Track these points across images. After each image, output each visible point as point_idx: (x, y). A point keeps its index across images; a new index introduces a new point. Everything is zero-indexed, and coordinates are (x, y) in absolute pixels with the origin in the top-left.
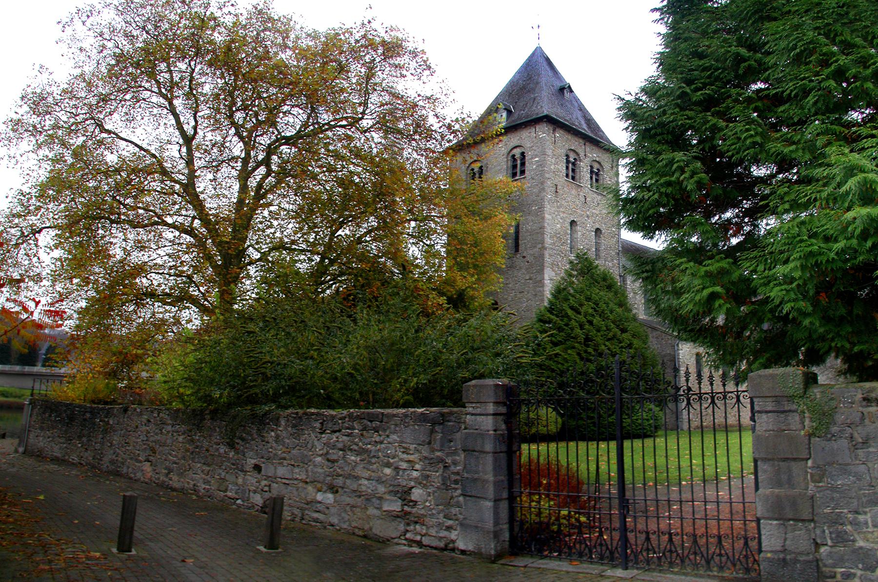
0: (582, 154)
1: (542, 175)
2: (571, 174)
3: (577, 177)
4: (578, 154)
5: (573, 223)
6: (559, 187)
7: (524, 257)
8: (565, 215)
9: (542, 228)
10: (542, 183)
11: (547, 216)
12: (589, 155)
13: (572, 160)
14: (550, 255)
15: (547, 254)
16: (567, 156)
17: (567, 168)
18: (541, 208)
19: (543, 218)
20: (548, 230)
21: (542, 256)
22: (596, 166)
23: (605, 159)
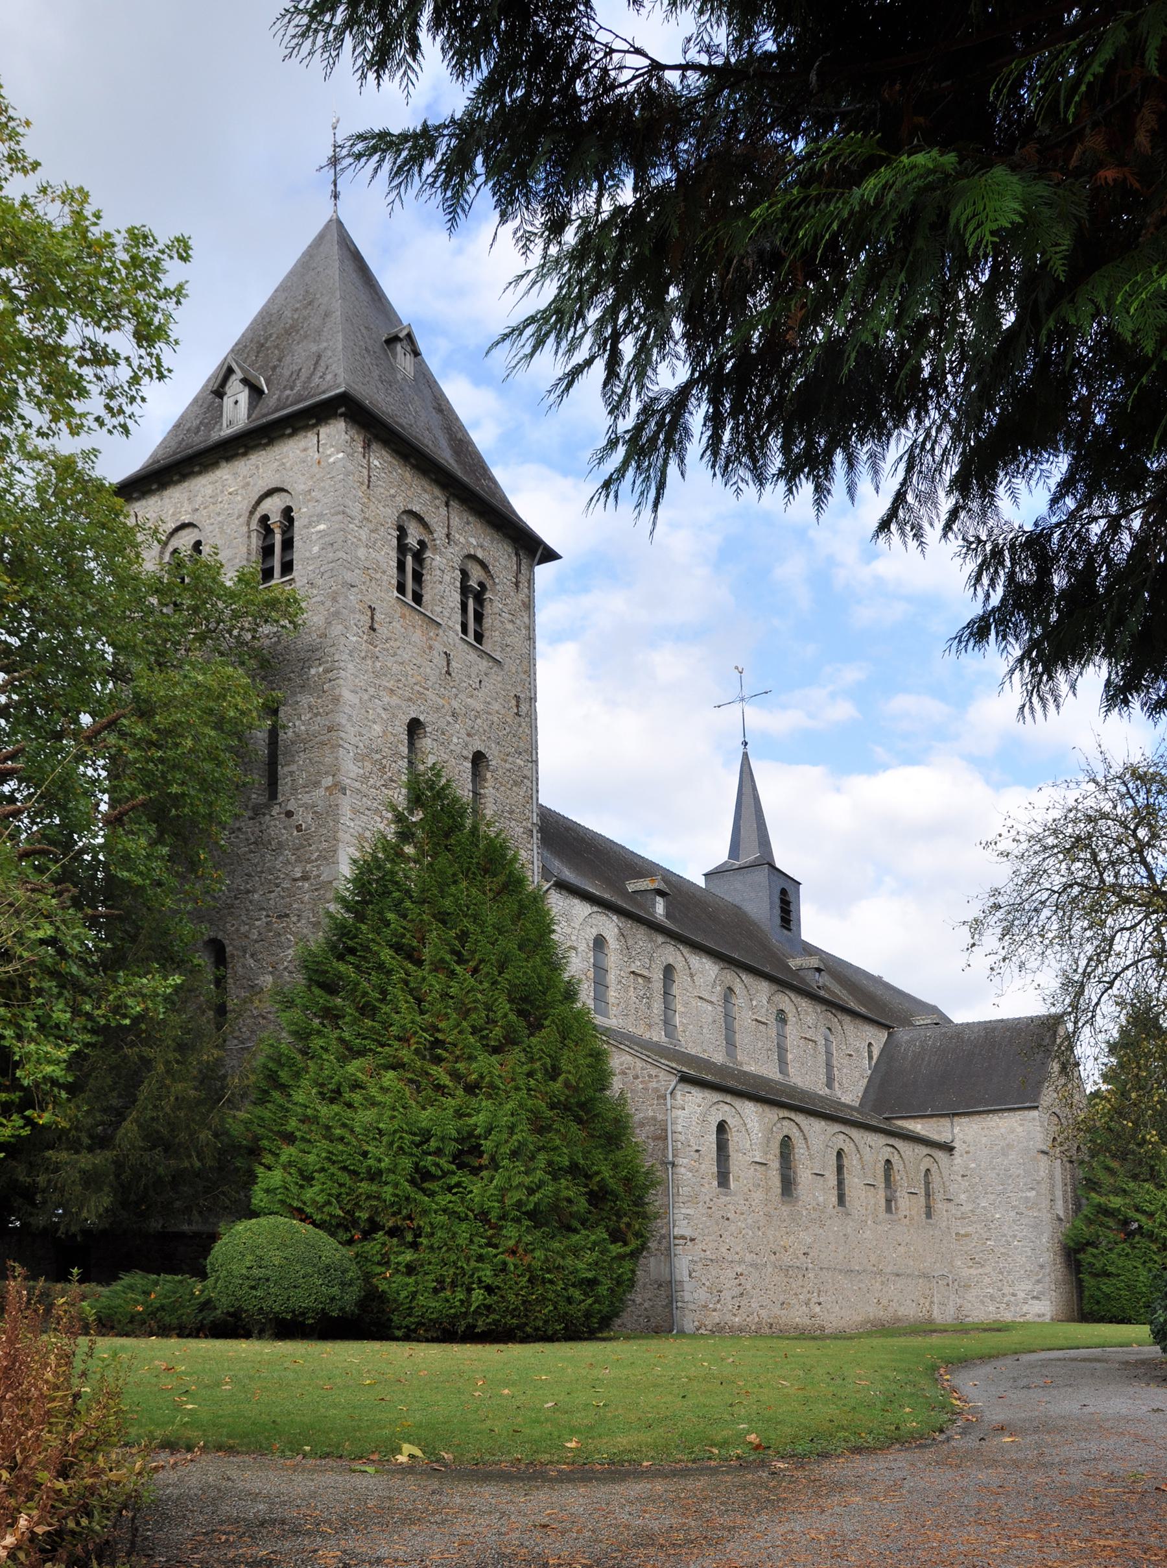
0: (440, 533)
5: (415, 727)
6: (378, 617)
7: (289, 814)
8: (395, 700)
11: (347, 695)
12: (457, 538)
13: (412, 541)
14: (355, 811)
15: (346, 804)
16: (402, 532)
17: (401, 566)
19: (336, 700)
20: (350, 733)
21: (333, 810)
22: (476, 574)
23: (500, 556)
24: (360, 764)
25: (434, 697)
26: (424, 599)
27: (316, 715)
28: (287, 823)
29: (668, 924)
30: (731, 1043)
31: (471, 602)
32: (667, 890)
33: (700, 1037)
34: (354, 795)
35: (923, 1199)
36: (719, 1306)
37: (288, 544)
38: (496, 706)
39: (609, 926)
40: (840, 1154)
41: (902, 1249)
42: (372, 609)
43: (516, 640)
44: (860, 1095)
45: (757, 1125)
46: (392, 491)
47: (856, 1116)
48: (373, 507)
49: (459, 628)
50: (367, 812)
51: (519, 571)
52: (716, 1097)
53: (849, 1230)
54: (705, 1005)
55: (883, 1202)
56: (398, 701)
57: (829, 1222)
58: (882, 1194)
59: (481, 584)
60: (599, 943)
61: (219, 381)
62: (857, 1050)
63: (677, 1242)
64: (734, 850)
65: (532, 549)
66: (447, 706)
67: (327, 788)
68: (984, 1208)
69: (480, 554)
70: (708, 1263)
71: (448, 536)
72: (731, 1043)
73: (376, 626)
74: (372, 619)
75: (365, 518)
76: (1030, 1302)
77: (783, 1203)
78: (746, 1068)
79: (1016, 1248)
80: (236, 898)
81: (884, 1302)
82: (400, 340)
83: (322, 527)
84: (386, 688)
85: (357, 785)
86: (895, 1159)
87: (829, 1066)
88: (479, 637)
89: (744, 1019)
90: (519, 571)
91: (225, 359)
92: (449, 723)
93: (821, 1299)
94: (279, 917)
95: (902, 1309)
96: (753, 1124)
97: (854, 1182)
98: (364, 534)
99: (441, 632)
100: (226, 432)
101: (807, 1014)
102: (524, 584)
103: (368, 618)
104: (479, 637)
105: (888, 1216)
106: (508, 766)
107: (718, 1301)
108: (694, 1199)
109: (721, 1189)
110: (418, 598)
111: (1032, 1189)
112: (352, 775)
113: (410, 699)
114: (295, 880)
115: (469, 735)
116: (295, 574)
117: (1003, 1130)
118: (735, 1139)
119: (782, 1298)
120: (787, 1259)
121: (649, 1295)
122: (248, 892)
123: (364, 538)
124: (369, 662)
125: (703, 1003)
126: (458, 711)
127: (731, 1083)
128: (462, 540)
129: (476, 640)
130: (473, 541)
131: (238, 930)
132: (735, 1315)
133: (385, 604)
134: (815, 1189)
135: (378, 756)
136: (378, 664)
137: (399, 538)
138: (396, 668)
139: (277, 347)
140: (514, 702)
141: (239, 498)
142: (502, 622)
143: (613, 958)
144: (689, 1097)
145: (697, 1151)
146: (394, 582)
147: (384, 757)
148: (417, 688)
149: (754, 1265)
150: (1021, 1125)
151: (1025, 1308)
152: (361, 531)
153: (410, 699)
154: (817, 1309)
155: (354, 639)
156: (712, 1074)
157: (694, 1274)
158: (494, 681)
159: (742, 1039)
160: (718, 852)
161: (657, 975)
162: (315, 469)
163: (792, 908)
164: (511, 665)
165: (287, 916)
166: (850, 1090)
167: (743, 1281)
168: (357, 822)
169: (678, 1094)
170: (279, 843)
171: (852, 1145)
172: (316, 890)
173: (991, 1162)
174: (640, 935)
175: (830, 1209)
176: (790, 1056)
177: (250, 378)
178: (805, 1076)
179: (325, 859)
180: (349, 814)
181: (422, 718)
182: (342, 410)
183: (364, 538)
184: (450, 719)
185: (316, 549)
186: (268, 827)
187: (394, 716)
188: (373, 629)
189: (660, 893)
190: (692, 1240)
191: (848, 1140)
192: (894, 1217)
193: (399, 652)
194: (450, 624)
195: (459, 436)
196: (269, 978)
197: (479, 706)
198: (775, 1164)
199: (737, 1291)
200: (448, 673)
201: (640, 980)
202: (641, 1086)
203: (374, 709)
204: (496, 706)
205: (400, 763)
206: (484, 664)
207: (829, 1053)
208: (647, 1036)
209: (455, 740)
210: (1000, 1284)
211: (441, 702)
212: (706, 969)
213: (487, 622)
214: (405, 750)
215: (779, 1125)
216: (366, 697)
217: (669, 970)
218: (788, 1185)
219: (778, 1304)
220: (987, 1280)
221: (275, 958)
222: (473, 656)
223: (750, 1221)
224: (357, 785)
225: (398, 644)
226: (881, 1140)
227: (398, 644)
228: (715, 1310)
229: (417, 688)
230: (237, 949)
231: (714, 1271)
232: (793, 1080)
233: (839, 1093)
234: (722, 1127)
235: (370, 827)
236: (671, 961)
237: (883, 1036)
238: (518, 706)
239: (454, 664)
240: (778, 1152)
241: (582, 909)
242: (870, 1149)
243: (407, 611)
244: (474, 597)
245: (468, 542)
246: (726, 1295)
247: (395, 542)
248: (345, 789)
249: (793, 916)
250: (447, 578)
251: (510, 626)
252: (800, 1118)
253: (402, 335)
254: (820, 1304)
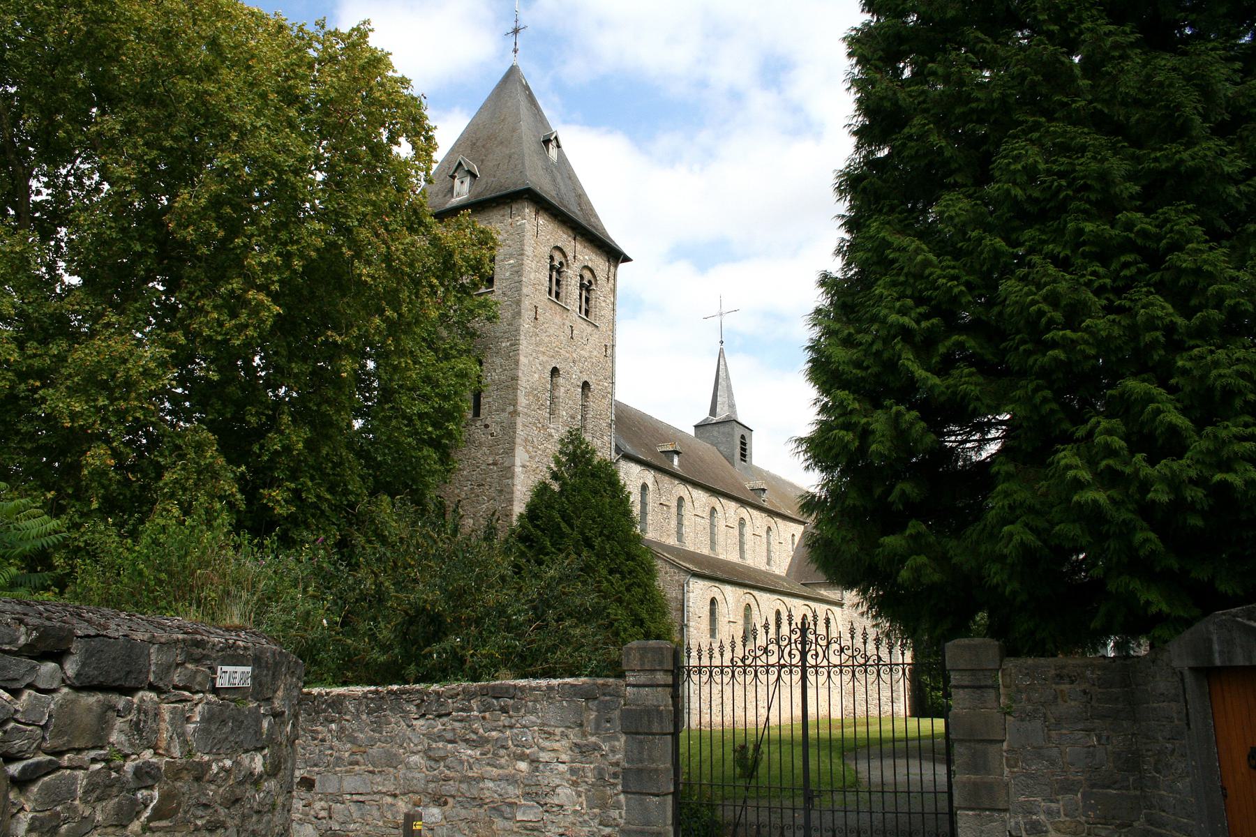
0: (570, 256)
1: (519, 290)
2: (554, 288)
3: (562, 295)
4: (565, 256)
5: (555, 371)
6: (539, 311)
8: (545, 358)
9: (515, 378)
10: (518, 303)
11: (523, 360)
14: (524, 426)
15: (520, 421)
16: (552, 258)
18: (515, 344)
19: (517, 362)
20: (523, 382)
21: (513, 426)
29: (681, 472)
38: (595, 353)
39: (649, 477)
43: (607, 312)
47: (785, 586)
52: (708, 583)
60: (644, 487)
72: (713, 543)
78: (721, 557)
87: (769, 551)
88: (587, 312)
104: (587, 312)
127: (719, 574)
138: (546, 340)
143: (651, 497)
158: (595, 339)
159: (720, 539)
161: (674, 504)
164: (603, 327)
166: (781, 566)
174: (666, 481)
178: (755, 560)
189: (677, 453)
197: (587, 355)
204: (595, 353)
206: (590, 329)
207: (769, 543)
212: (700, 496)
213: (592, 303)
214: (549, 386)
217: (681, 499)
222: (585, 325)
241: (635, 469)
244: (586, 287)
249: (748, 453)
252: (755, 593)
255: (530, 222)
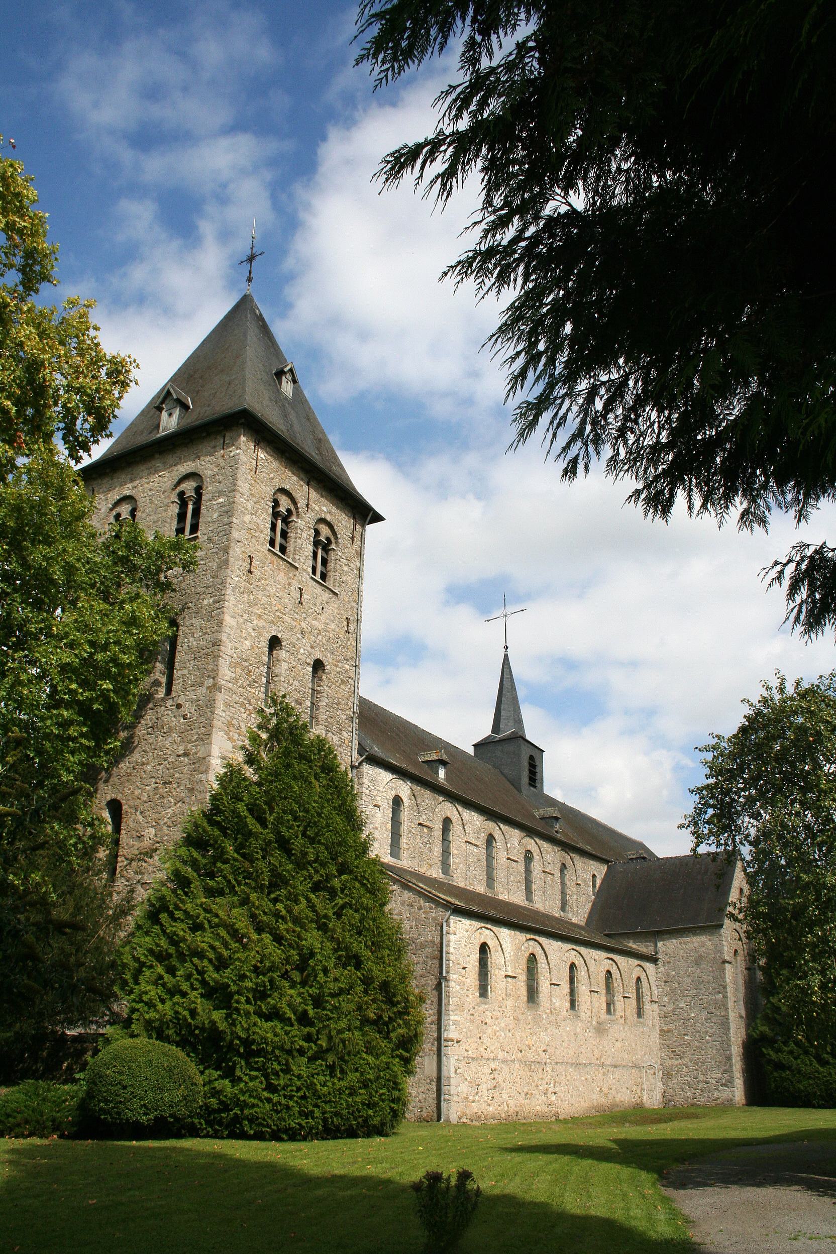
0: (302, 503)
1: (228, 534)
2: (278, 540)
3: (290, 549)
4: (294, 502)
5: (275, 643)
6: (255, 563)
7: (179, 706)
8: (261, 623)
9: (217, 643)
10: (226, 549)
11: (228, 619)
12: (316, 506)
13: (282, 509)
14: (227, 705)
15: (221, 698)
16: (276, 503)
17: (273, 527)
18: (219, 601)
19: (220, 623)
20: (227, 648)
21: (211, 704)
22: (325, 531)
24: (233, 670)
25: (289, 620)
26: (288, 550)
27: (205, 634)
28: (177, 714)
29: (447, 786)
30: (490, 880)
31: (320, 552)
32: (448, 760)
33: (467, 875)
34: (227, 693)
35: (634, 1002)
36: (477, 1098)
37: (197, 513)
38: (333, 626)
39: (404, 789)
40: (573, 966)
41: (618, 1044)
42: (251, 558)
43: (350, 578)
44: (586, 916)
45: (509, 945)
46: (272, 475)
47: (584, 935)
48: (257, 486)
49: (310, 570)
50: (235, 705)
51: (355, 529)
53: (578, 1030)
54: (472, 848)
55: (604, 1005)
56: (264, 624)
57: (563, 1023)
58: (603, 998)
59: (328, 539)
60: (397, 801)
61: (160, 400)
62: (584, 880)
63: (446, 1044)
64: (496, 728)
65: (364, 514)
66: (298, 627)
67: (208, 688)
68: (682, 1008)
69: (328, 518)
70: (469, 1060)
71: (307, 506)
72: (490, 880)
73: (253, 569)
74: (250, 564)
75: (252, 494)
76: (720, 1088)
77: (529, 1008)
78: (501, 897)
79: (707, 1042)
80: (134, 769)
81: (605, 1090)
82: (285, 373)
83: (221, 500)
84: (256, 613)
85: (230, 685)
86: (614, 970)
87: (563, 893)
88: (324, 576)
89: (501, 857)
90: (355, 529)
91: (166, 385)
92: (298, 639)
93: (557, 1089)
94: (164, 784)
95: (619, 1095)
96: (509, 945)
97: (583, 989)
98: (249, 505)
99: (297, 573)
100: (162, 433)
101: (548, 853)
102: (358, 539)
103: (247, 565)
104: (324, 576)
105: (608, 1017)
106: (338, 670)
107: (477, 1093)
108: (461, 1007)
109: (481, 999)
110: (283, 549)
111: (719, 992)
112: (226, 678)
113: (273, 622)
114: (178, 756)
115: (312, 647)
116: (199, 534)
117: (696, 945)
118: (495, 958)
119: (526, 1090)
120: (530, 1056)
121: (422, 1089)
122: (143, 764)
123: (249, 507)
124: (245, 595)
125: (469, 849)
126: (305, 630)
127: (492, 913)
128: (317, 508)
129: (321, 578)
130: (324, 508)
131: (133, 793)
132: (489, 1105)
133: (260, 554)
134: (553, 996)
135: (246, 664)
136: (252, 597)
137: (274, 508)
138: (264, 600)
139: (201, 377)
140: (345, 623)
141: (166, 479)
142: (341, 566)
143: (406, 814)
144: (459, 925)
145: (464, 968)
146: (268, 538)
147: (251, 665)
148: (278, 614)
149: (505, 1061)
150: (710, 940)
151: (716, 1093)
152: (248, 503)
153: (273, 622)
154: (553, 1098)
155: (237, 579)
156: (478, 905)
157: (458, 1071)
158: (334, 605)
159: (500, 874)
160: (484, 729)
161: (438, 826)
162: (221, 461)
163: (537, 770)
164: (344, 596)
165: (170, 783)
166: (579, 914)
167: (496, 1076)
168: (228, 713)
169: (452, 922)
170: (170, 728)
171: (581, 959)
172: (194, 763)
173: (687, 971)
174: (427, 796)
175: (564, 1014)
176: (534, 887)
177: (181, 398)
178: (545, 903)
179: (202, 740)
180: (222, 707)
181: (279, 636)
182: (243, 420)
183: (249, 507)
184: (299, 636)
185: (215, 516)
186: (163, 716)
187: (260, 634)
188: (250, 572)
189: (443, 763)
190: (458, 1042)
191: (578, 955)
192: (612, 1017)
193: (267, 588)
194: (305, 567)
195: (320, 436)
196: (152, 831)
197: (321, 626)
198: (523, 977)
199: (491, 1084)
200: (300, 603)
201: (425, 830)
202: (423, 916)
203: (246, 629)
204: (333, 626)
205: (262, 668)
206: (326, 595)
207: (563, 884)
208: (428, 874)
209: (302, 651)
210: (695, 1072)
211: (294, 623)
212: (474, 819)
213: (331, 565)
214: (266, 659)
215: (526, 945)
216: (241, 621)
217: (447, 822)
218: (532, 994)
219: (523, 1094)
220: (685, 1069)
221: (158, 816)
222: (319, 589)
223: (503, 1025)
224: (230, 685)
225: (267, 582)
226: (604, 955)
227: (267, 582)
228: (473, 1102)
229: (278, 614)
230: (131, 807)
231: (474, 1066)
232: (537, 906)
233: (570, 916)
234: (484, 949)
235: (236, 716)
236: (449, 815)
237: (604, 868)
238: (348, 626)
239: (305, 596)
240: (525, 967)
241: (385, 776)
242: (597, 961)
243: (275, 559)
244: (323, 546)
245: (321, 509)
246: (483, 1088)
247: (271, 510)
248: (220, 688)
249: (538, 776)
250: (305, 535)
251: (346, 568)
252: (542, 940)
253: (286, 369)
254: (555, 1093)
255: (245, 452)
